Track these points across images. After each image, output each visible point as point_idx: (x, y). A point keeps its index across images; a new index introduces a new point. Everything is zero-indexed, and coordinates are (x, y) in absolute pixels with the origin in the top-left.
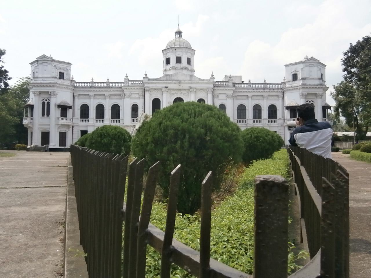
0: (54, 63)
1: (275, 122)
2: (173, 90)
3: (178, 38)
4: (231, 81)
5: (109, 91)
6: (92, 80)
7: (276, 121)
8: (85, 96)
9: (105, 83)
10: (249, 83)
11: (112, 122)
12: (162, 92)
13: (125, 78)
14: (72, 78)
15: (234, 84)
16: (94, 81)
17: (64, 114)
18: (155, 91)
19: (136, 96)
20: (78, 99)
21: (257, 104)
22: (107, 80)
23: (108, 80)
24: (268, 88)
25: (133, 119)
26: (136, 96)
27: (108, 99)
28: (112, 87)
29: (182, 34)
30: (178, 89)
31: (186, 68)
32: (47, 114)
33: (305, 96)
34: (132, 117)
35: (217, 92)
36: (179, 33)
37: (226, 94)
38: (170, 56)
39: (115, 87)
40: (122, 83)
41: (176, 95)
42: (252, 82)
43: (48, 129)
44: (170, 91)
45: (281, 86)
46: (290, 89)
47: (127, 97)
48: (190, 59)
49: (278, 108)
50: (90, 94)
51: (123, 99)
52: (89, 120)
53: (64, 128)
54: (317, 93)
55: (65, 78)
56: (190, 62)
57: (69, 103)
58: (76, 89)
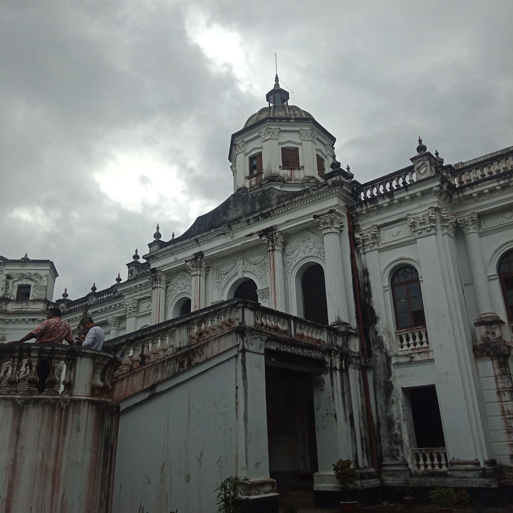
0: (7, 267)
4: (421, 163)
6: (94, 288)
16: (97, 291)
19: (149, 305)
22: (116, 280)
26: (149, 305)
35: (367, 225)
37: (405, 219)
55: (31, 298)
56: (299, 158)
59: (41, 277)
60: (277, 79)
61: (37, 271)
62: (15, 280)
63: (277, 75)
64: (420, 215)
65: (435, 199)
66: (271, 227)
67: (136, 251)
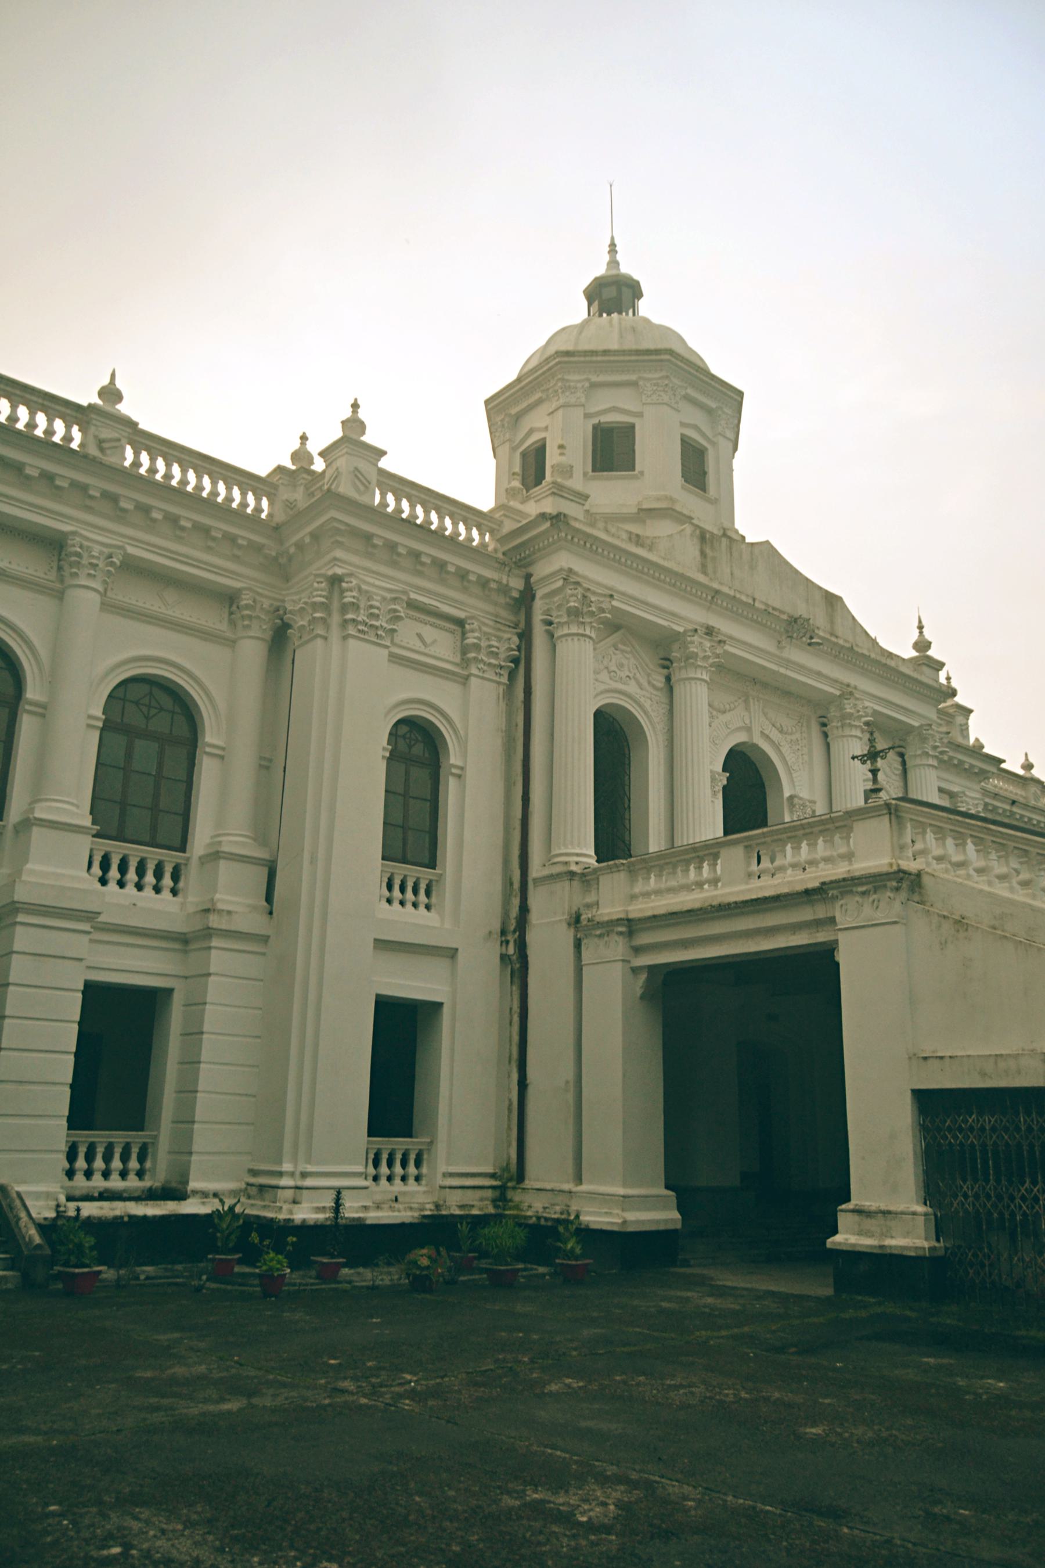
5: (121, 516)
18: (611, 640)
23: (111, 393)
27: (85, 600)
36: (613, 294)
38: (640, 415)
47: (372, 632)
51: (252, 651)
60: (613, 246)
63: (612, 238)
67: (355, 406)
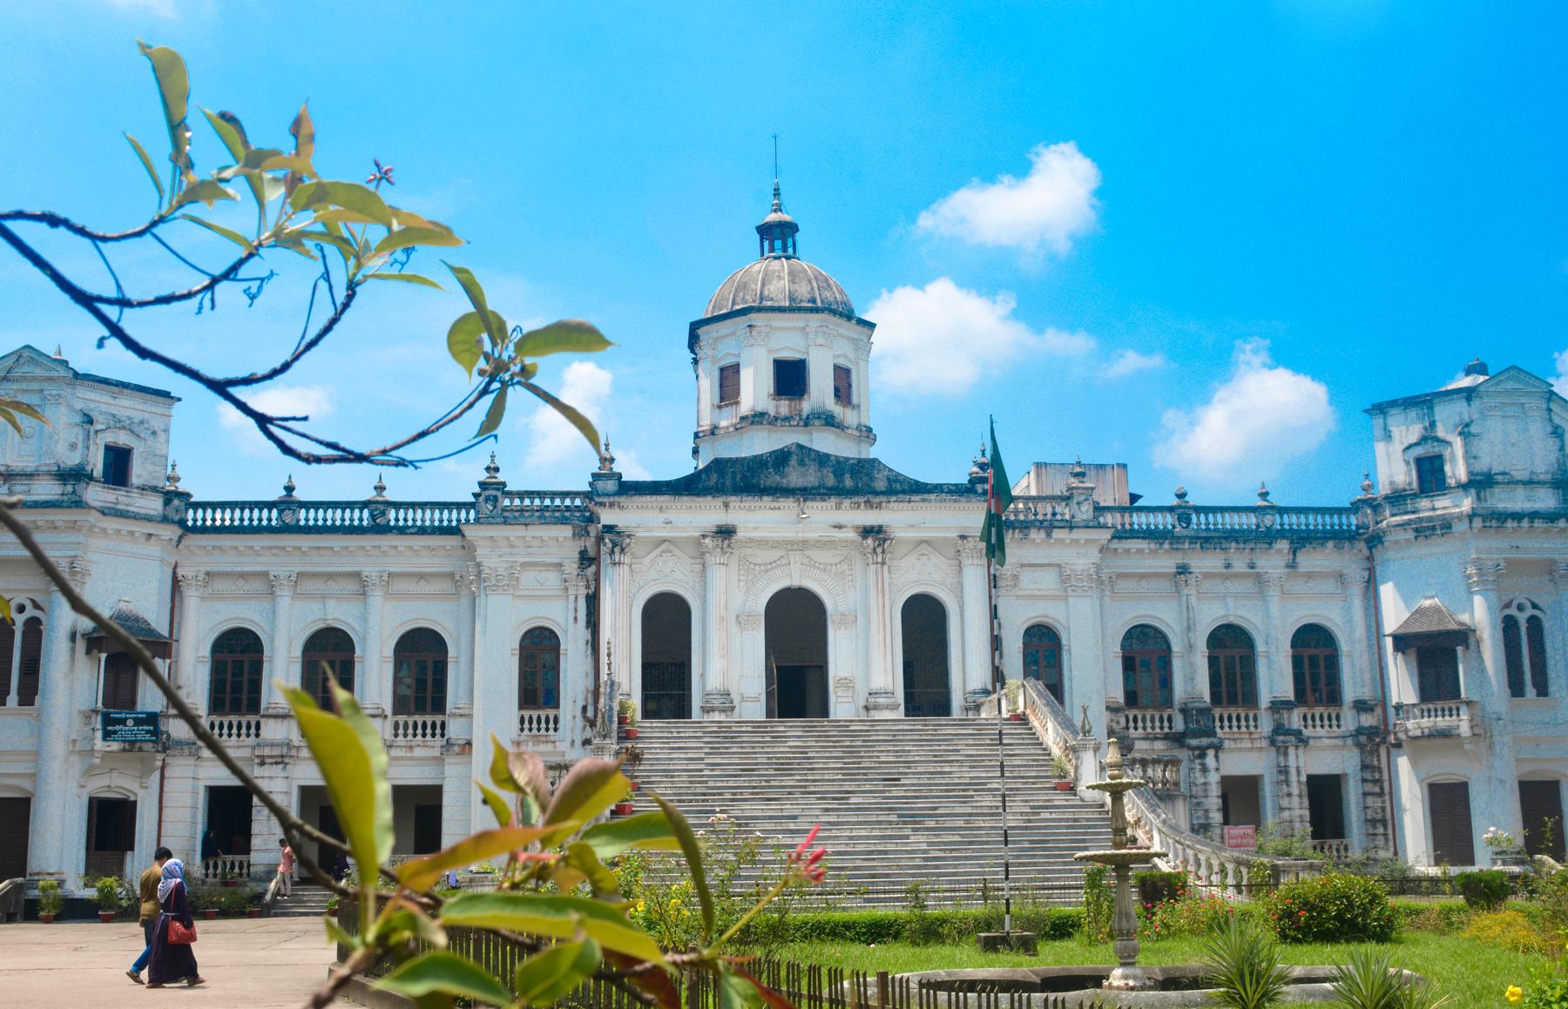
1: (1334, 722)
2: (762, 543)
3: (778, 258)
5: (385, 554)
6: (290, 489)
7: (1338, 718)
8: (241, 583)
9: (364, 505)
10: (1180, 507)
11: (396, 735)
12: (701, 555)
13: (483, 476)
14: (173, 479)
15: (1099, 510)
16: (299, 495)
17: (118, 695)
18: (658, 551)
20: (202, 598)
21: (1232, 620)
24: (1282, 534)
25: (526, 714)
27: (376, 599)
28: (402, 531)
29: (798, 236)
30: (792, 543)
31: (830, 421)
32: (20, 693)
33: (1494, 577)
34: (521, 707)
37: (1059, 566)
39: (422, 531)
40: (459, 506)
41: (778, 572)
42: (1193, 500)
43: (26, 784)
44: (748, 551)
45: (1353, 520)
46: (1407, 541)
48: (848, 371)
49: (1344, 646)
50: (273, 571)
51: (465, 601)
52: (263, 722)
53: (115, 774)
54: (1554, 562)
56: (850, 386)
57: (154, 625)
58: (193, 540)
59: (154, 433)
61: (147, 416)
62: (99, 427)
64: (1079, 568)
65: (1096, 553)
66: (880, 527)
67: (493, 457)
